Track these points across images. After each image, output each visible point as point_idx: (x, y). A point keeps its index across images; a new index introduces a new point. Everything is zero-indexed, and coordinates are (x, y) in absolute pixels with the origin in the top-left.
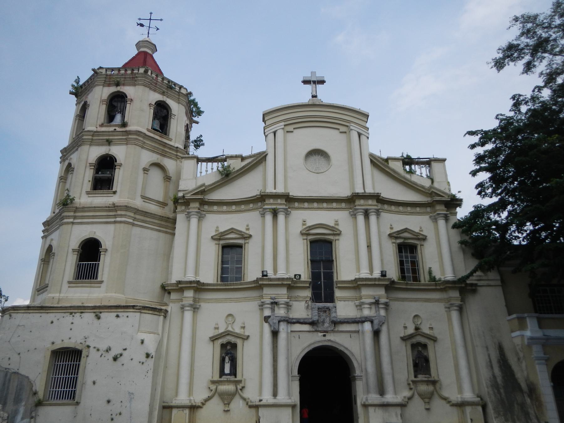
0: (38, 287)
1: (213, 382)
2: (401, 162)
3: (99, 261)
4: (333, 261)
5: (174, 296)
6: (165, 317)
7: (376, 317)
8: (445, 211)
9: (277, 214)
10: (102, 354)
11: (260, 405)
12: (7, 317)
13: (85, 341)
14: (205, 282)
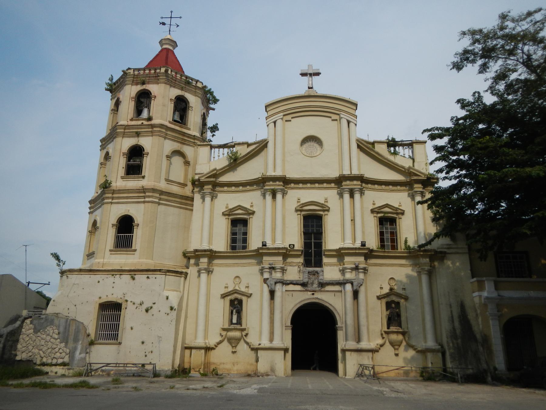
0: (87, 253)
1: (224, 330)
2: (386, 144)
3: (133, 233)
4: (322, 232)
5: (192, 261)
6: (186, 278)
7: (355, 279)
8: (422, 189)
9: (276, 193)
10: (137, 307)
11: (259, 348)
12: (65, 277)
13: (124, 297)
14: (217, 250)
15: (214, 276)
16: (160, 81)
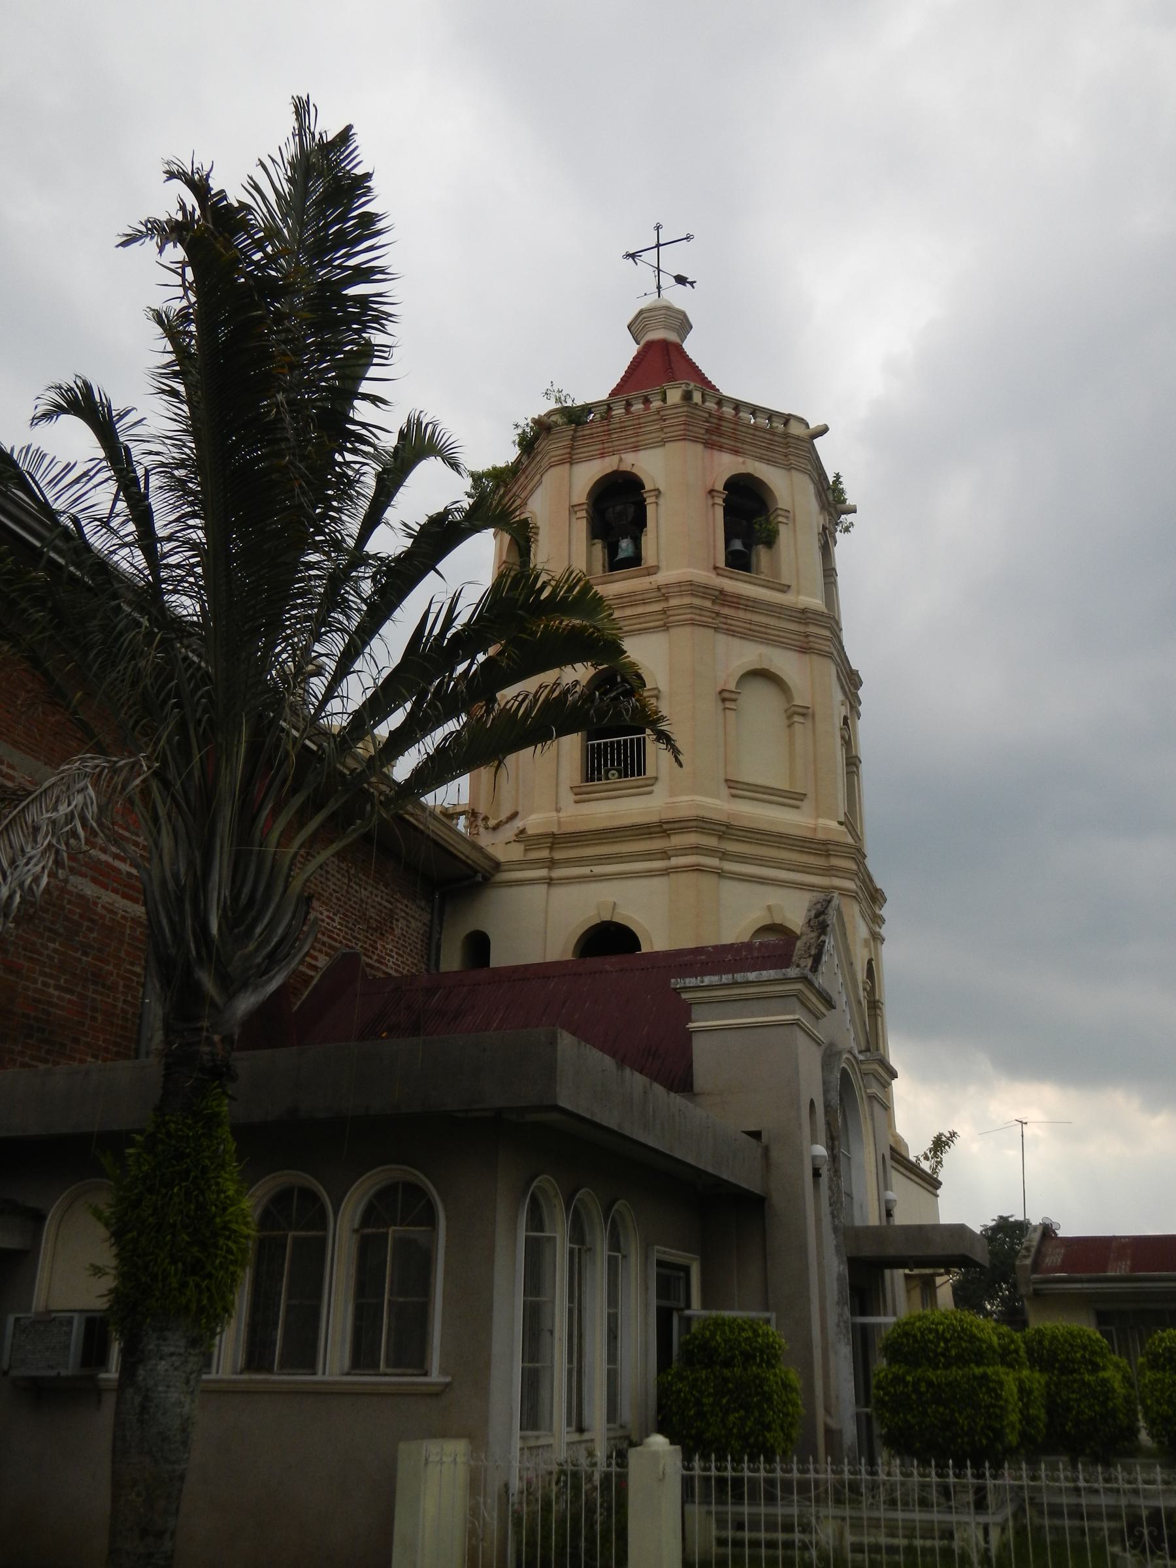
16: (668, 435)
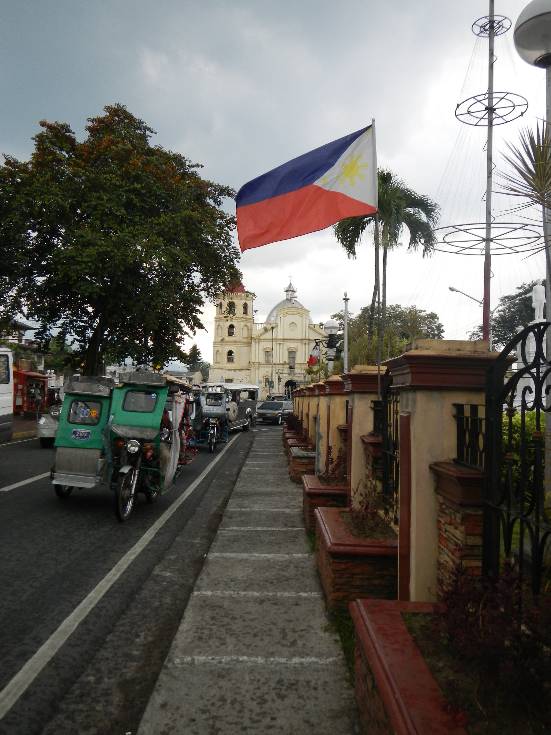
15: (260, 371)
